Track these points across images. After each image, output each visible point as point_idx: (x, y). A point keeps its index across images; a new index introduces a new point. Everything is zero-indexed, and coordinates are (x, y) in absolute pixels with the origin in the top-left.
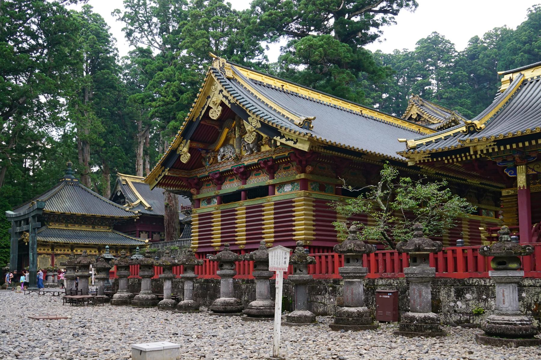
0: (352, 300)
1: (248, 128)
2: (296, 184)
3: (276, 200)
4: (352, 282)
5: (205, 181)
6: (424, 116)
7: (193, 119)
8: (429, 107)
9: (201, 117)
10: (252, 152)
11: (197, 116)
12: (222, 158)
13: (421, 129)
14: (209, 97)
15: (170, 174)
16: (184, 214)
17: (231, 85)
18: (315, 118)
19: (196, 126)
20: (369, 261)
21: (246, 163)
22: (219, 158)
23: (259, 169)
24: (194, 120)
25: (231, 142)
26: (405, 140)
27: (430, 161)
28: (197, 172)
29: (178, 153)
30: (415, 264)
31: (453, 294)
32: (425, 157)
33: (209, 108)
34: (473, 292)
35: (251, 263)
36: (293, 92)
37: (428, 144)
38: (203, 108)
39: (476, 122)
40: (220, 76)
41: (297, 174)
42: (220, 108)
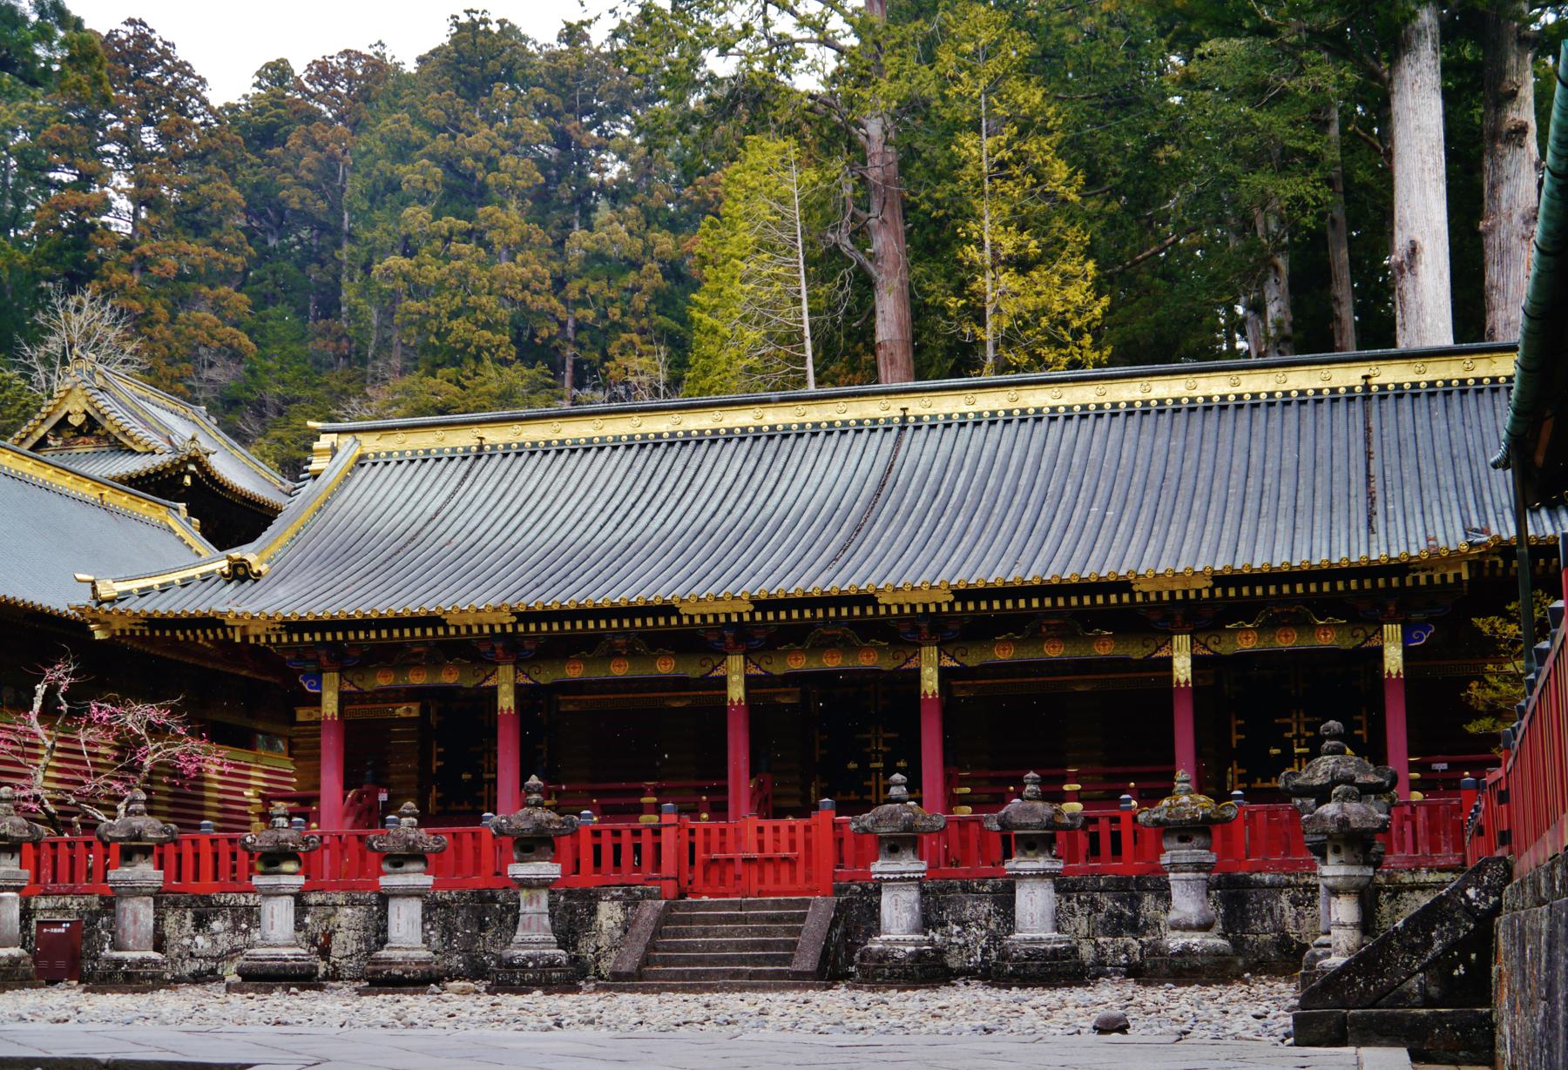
6: (107, 425)
20: (38, 859)
26: (91, 578)
31: (189, 922)
34: (225, 918)
37: (144, 592)
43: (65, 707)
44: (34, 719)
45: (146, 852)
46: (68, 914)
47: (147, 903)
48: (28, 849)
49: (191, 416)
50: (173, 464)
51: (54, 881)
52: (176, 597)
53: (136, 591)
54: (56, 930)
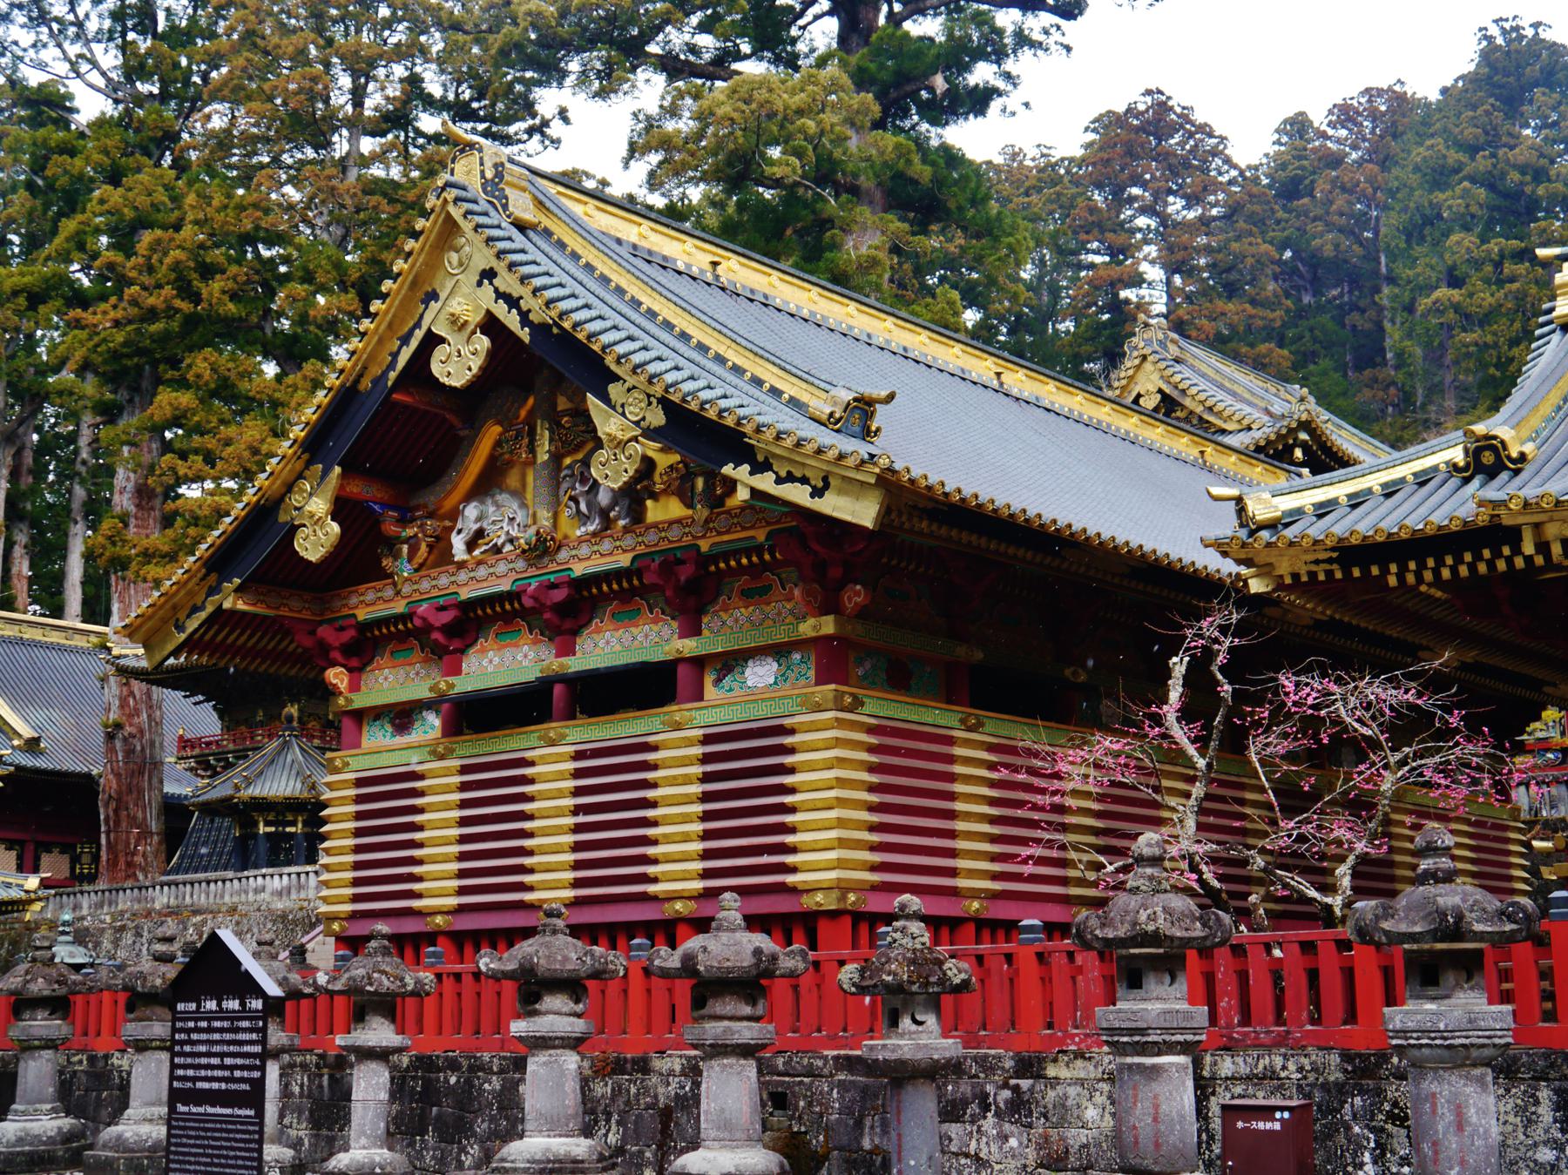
0: (1157, 1145)
1: (609, 425)
2: (797, 656)
3: (711, 721)
4: (1156, 1069)
5: (390, 637)
6: (1187, 402)
7: (357, 381)
8: (1204, 368)
9: (393, 375)
10: (607, 523)
11: (376, 371)
12: (471, 545)
13: (1209, 450)
14: (433, 296)
15: (241, 606)
16: (191, 769)
17: (533, 254)
18: (891, 397)
19: (373, 405)
21: (579, 570)
22: (458, 543)
23: (634, 592)
24: (366, 384)
25: (512, 480)
26: (1234, 492)
27: (1339, 575)
28: (354, 600)
29: (283, 518)
30: (1432, 992)
31: (1546, 1113)
32: (1317, 562)
33: (432, 340)
35: (683, 988)
36: (752, 291)
38: (405, 340)
39: (1505, 433)
40: (486, 214)
41: (804, 618)
42: (483, 343)
43: (1226, 689)
44: (1171, 717)
45: (1469, 966)
46: (1279, 1089)
47: (1481, 1081)
48: (1192, 955)
49: (1282, 393)
50: (1279, 436)
51: (1246, 1020)
52: (1383, 510)
53: (1309, 509)
54: (1261, 1125)
